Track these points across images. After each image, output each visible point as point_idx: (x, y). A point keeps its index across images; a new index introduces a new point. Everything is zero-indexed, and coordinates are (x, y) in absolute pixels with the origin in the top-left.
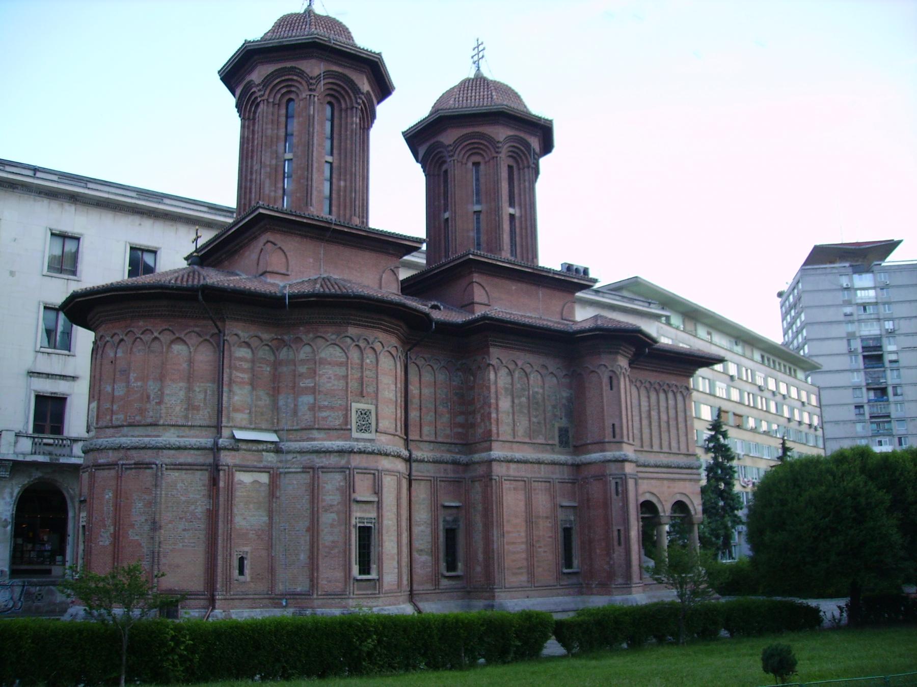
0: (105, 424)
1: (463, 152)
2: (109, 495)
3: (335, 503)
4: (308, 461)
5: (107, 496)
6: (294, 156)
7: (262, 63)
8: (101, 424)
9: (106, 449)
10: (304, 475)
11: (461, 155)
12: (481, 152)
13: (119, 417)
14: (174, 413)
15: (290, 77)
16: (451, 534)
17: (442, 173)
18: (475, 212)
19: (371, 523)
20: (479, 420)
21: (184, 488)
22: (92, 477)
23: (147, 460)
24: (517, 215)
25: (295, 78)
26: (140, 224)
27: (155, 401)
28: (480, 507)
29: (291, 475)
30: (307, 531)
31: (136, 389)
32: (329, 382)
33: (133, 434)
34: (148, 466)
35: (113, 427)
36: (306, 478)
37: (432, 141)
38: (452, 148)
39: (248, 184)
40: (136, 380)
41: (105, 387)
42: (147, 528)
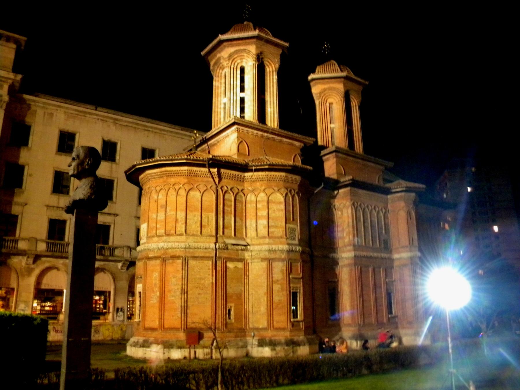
0: (152, 235)
2: (156, 275)
7: (228, 47)
8: (149, 235)
9: (153, 250)
10: (262, 263)
13: (161, 231)
14: (192, 229)
20: (345, 235)
21: (198, 270)
22: (145, 264)
23: (178, 255)
26: (148, 136)
27: (181, 222)
29: (255, 264)
33: (169, 241)
34: (178, 257)
36: (264, 264)
40: (170, 210)
42: (179, 293)
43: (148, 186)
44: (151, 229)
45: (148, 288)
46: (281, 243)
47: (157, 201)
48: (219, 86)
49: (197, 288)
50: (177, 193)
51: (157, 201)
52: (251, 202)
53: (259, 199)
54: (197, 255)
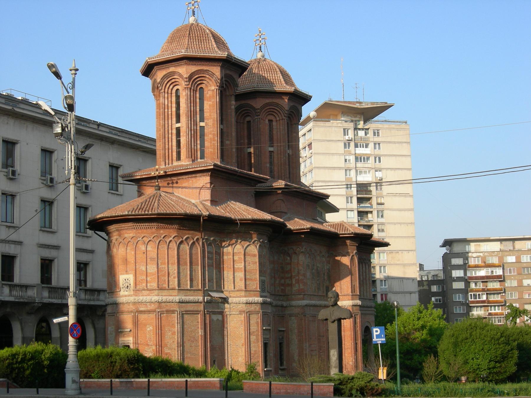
0: (141, 288)
1: (264, 113)
3: (255, 331)
4: (242, 308)
5: (148, 329)
6: (206, 125)
11: (263, 115)
12: (274, 114)
13: (152, 284)
15: (204, 75)
16: (281, 344)
17: (246, 122)
18: (270, 151)
19: (267, 341)
20: (294, 282)
24: (291, 154)
25: (207, 76)
27: (173, 276)
28: (296, 331)
30: (242, 345)
31: (162, 269)
32: (250, 266)
35: (148, 290)
37: (243, 102)
38: (259, 111)
39: (170, 136)
40: (161, 264)
41: (139, 267)
42: (175, 345)
43: (131, 235)
44: (140, 281)
45: (141, 341)
46: (255, 296)
47: (146, 252)
48: (170, 105)
49: (189, 340)
50: (168, 246)
51: (145, 253)
52: (228, 254)
53: (235, 251)
54: (187, 309)
